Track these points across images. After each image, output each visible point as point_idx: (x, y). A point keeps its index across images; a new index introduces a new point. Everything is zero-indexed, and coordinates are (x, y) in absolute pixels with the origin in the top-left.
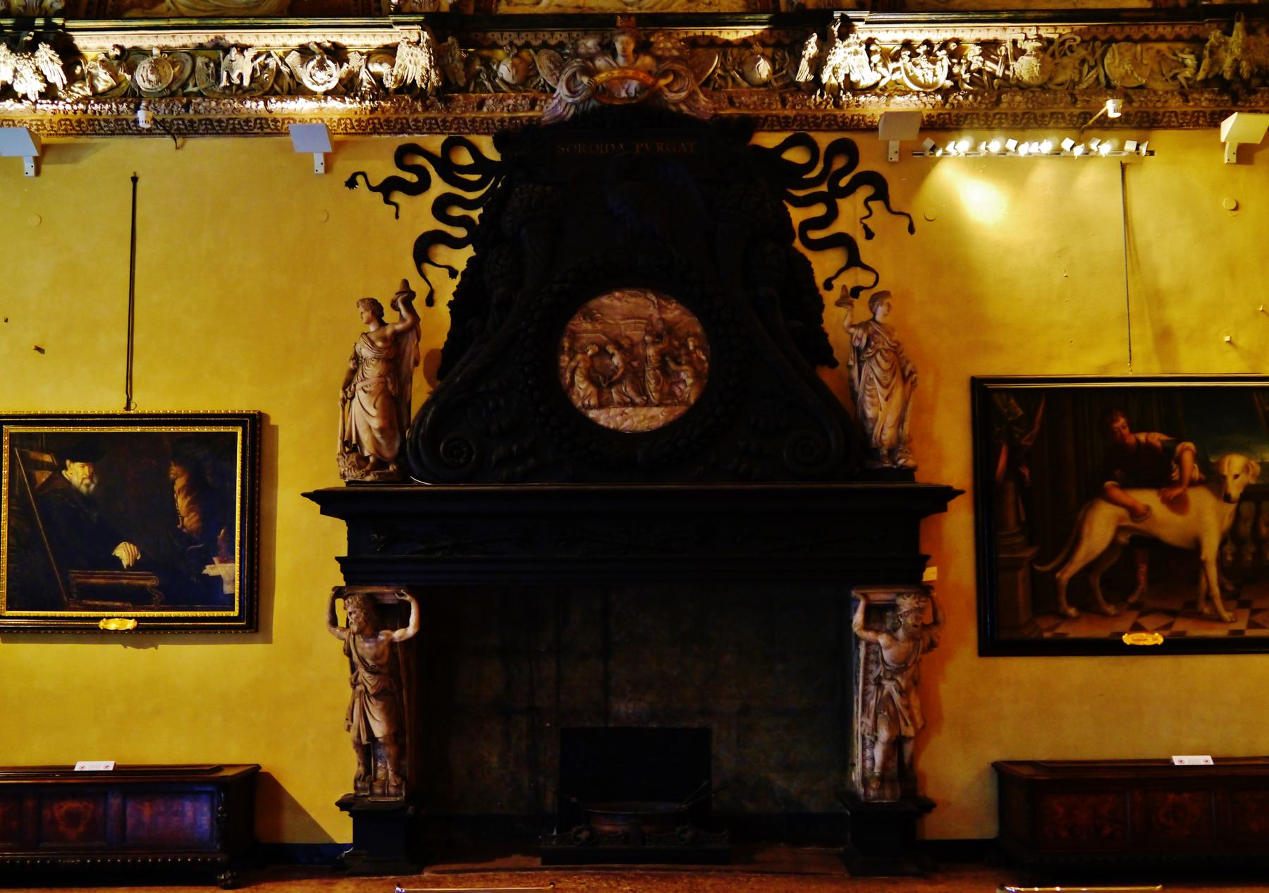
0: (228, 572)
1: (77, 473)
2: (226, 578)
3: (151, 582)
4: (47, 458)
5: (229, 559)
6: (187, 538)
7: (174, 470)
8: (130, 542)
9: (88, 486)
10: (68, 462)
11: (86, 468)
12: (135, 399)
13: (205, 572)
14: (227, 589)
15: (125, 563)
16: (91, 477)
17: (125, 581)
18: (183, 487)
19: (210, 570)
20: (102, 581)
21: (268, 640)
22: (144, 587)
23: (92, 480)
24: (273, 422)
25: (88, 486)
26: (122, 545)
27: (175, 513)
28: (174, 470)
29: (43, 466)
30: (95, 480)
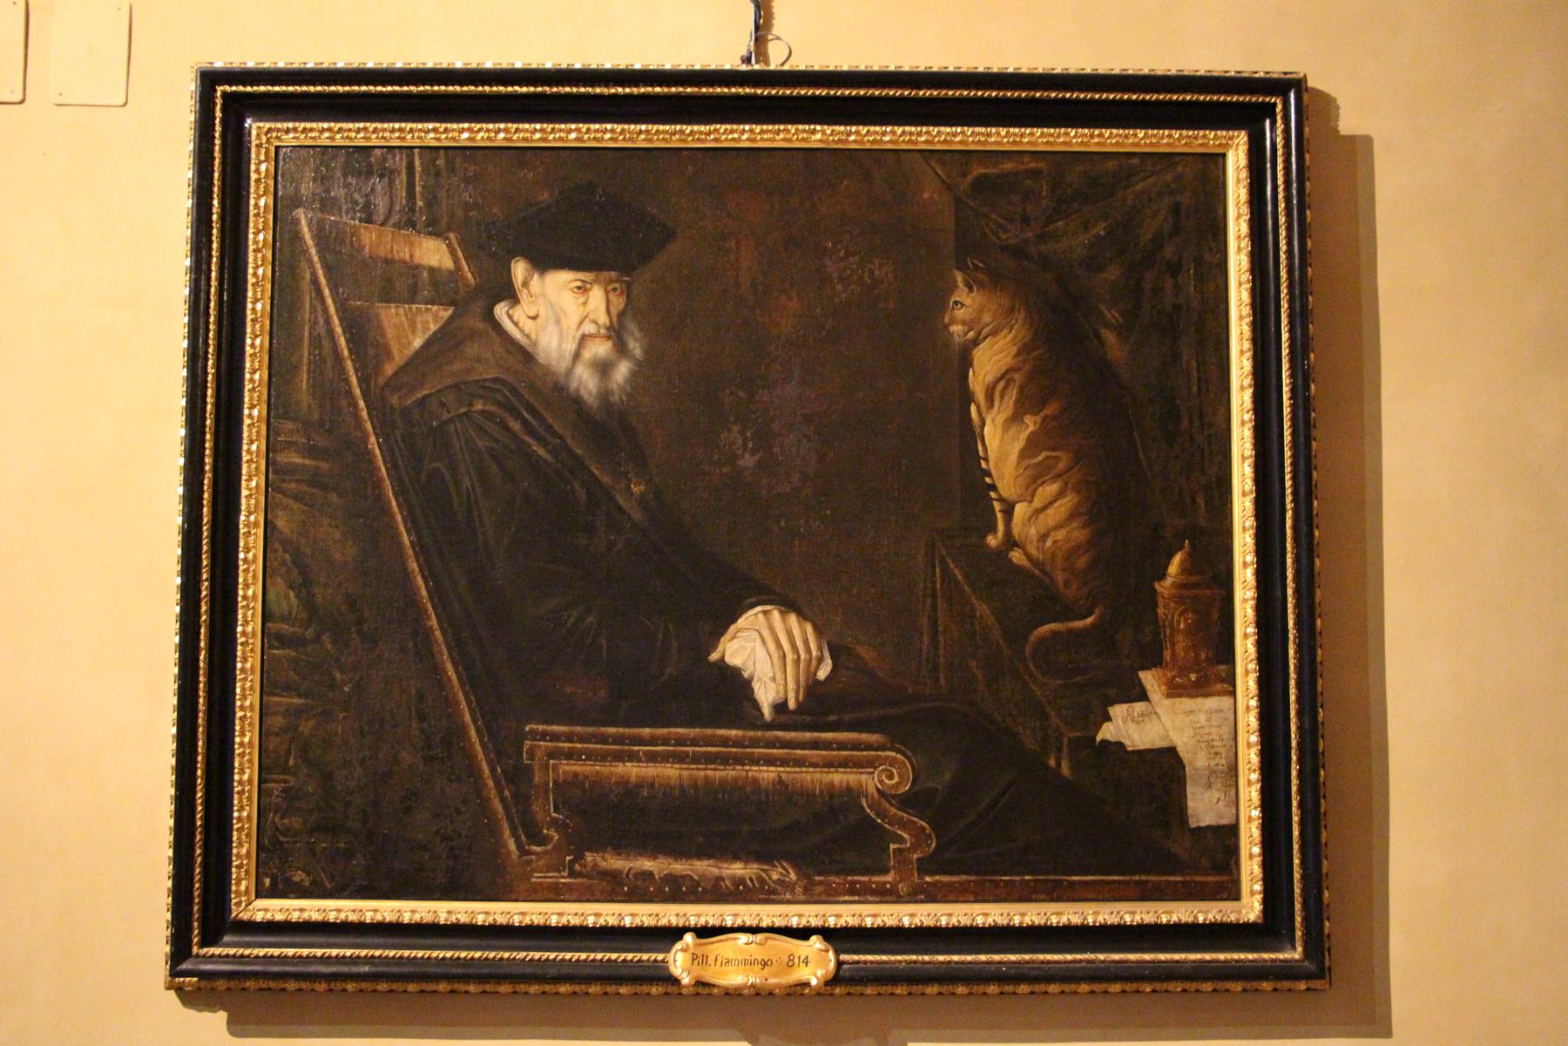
0: (1202, 732)
1: (561, 317)
2: (1196, 760)
3: (877, 776)
4: (434, 253)
5: (1209, 670)
6: (1028, 593)
7: (967, 306)
8: (788, 605)
9: (603, 368)
10: (519, 269)
11: (597, 296)
12: (779, 26)
13: (1107, 732)
14: (1203, 807)
15: (766, 695)
16: (615, 332)
17: (767, 774)
18: (1005, 376)
19: (1127, 727)
20: (671, 772)
21: (1387, 1032)
22: (851, 795)
23: (621, 349)
24: (1349, 123)
25: (603, 368)
26: (752, 619)
27: (975, 488)
28: (967, 306)
29: (408, 284)
30: (636, 347)
